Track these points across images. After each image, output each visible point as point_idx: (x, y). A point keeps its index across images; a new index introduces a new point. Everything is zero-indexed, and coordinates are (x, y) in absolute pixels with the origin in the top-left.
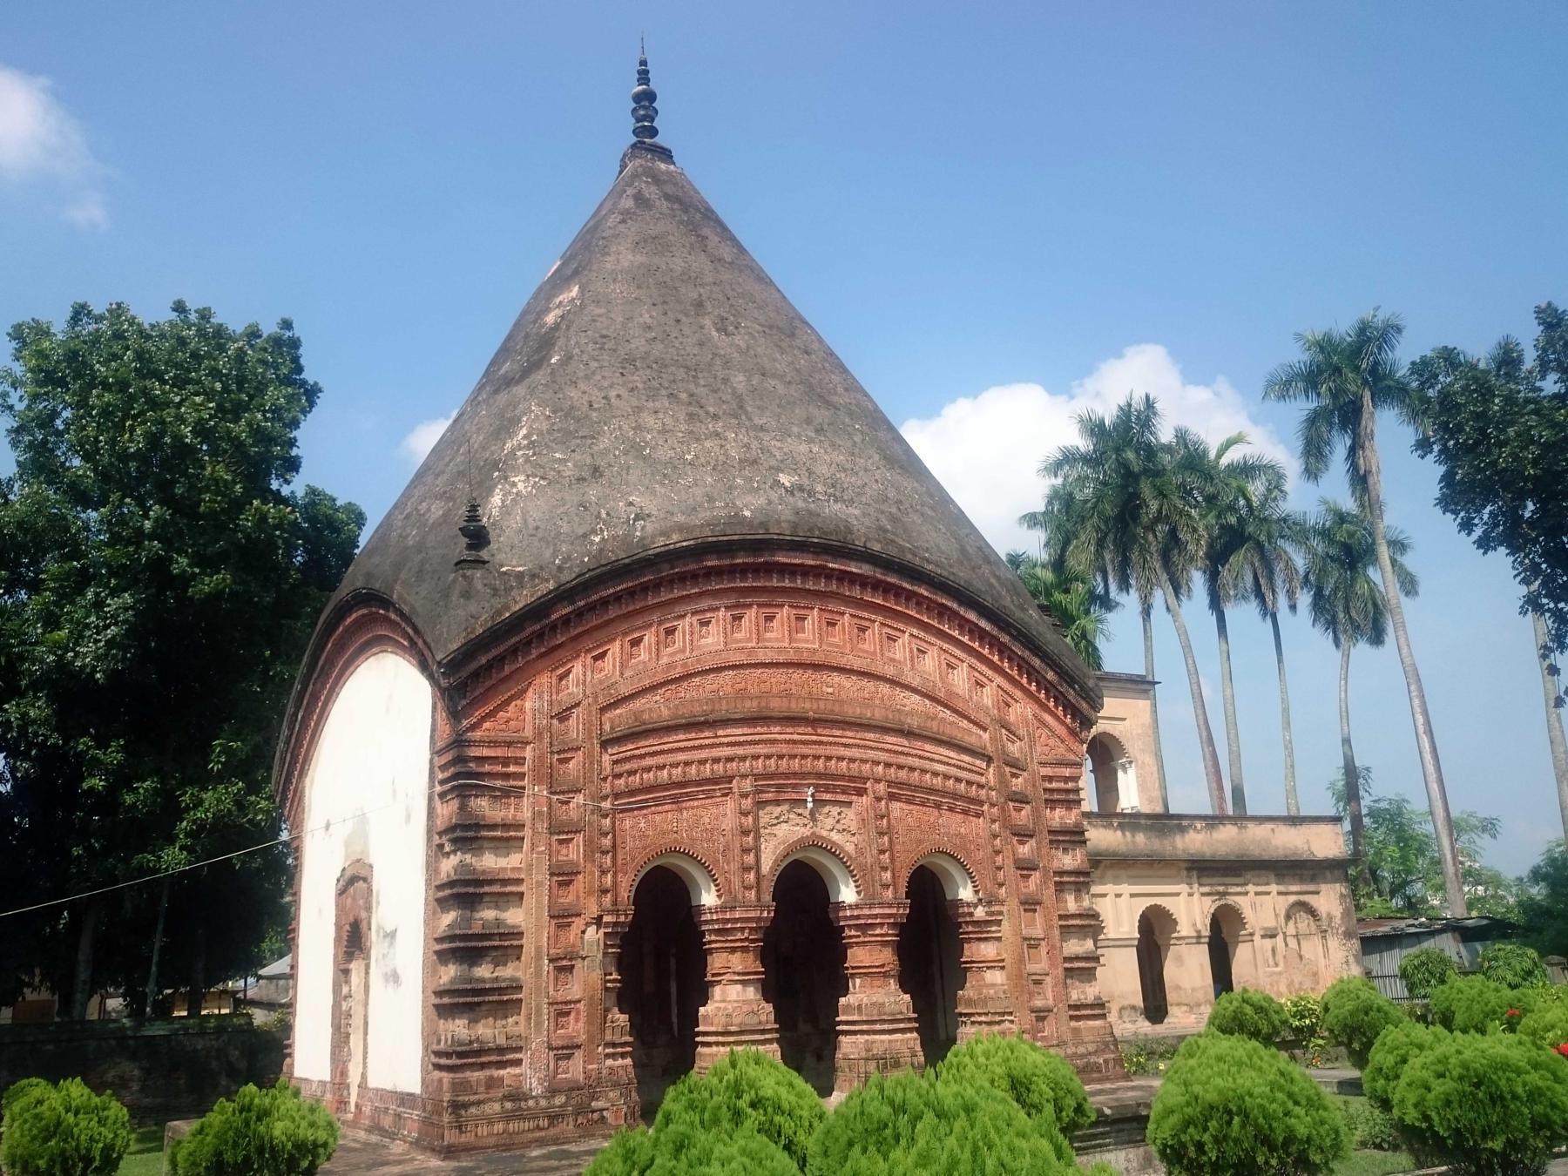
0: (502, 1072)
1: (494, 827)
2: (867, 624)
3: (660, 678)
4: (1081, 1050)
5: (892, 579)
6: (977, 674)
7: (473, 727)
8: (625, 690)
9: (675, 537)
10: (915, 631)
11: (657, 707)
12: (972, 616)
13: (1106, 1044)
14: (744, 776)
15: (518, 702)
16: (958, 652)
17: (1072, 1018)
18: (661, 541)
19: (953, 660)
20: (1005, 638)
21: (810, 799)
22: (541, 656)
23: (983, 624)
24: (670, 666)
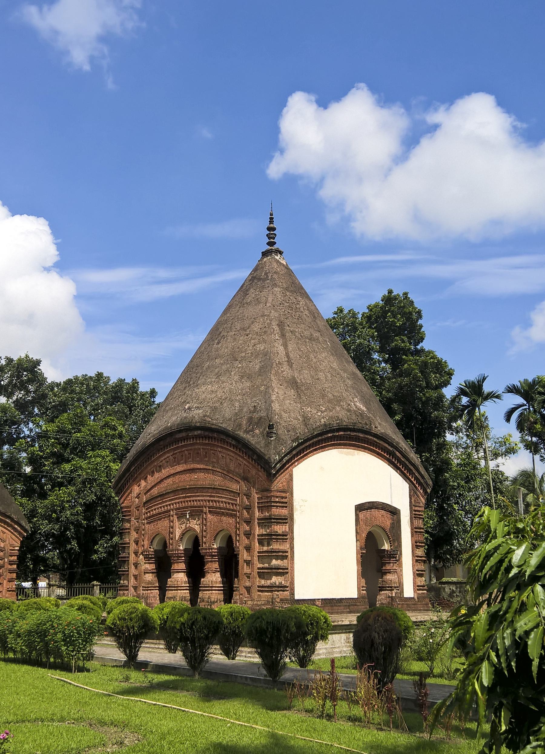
0: (126, 592)
1: (126, 529)
2: (206, 451)
3: (156, 482)
4: (259, 603)
5: (207, 433)
6: (238, 461)
7: (123, 503)
8: (149, 487)
9: (151, 439)
10: (219, 449)
11: (155, 491)
12: (230, 440)
13: (268, 601)
14: (172, 510)
15: (131, 495)
16: (233, 455)
17: (259, 591)
18: (149, 441)
19: (231, 458)
20: (240, 446)
21: (188, 515)
22: (133, 481)
23: (233, 442)
24: (158, 478)
